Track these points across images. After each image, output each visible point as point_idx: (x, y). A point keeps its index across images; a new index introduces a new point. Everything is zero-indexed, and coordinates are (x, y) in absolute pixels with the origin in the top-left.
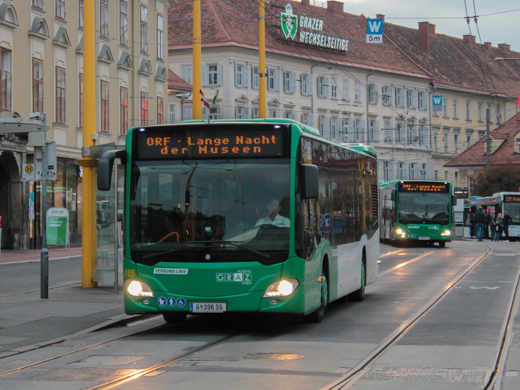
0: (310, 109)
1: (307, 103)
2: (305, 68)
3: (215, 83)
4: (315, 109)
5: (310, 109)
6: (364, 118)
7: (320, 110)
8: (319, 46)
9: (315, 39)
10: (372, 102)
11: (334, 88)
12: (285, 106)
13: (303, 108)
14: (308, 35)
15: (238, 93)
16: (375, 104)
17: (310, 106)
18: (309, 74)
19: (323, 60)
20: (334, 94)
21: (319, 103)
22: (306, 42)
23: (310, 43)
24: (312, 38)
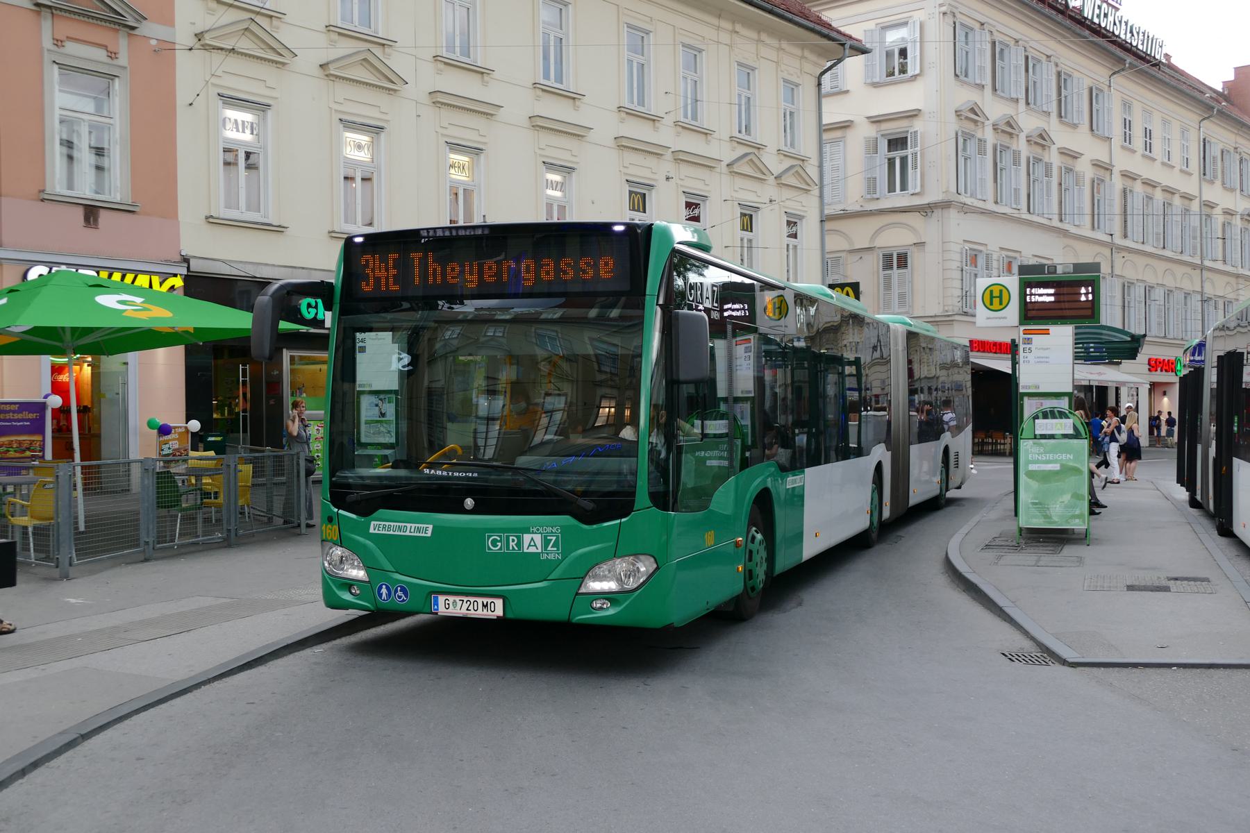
3: (903, 70)
4: (1116, 171)
5: (1108, 168)
6: (1195, 206)
7: (1126, 175)
9: (1111, 18)
10: (1207, 177)
11: (1148, 133)
12: (1064, 152)
14: (1099, 7)
15: (964, 96)
16: (1212, 182)
18: (1106, 89)
20: (1148, 147)
22: (1096, 20)
23: (1103, 25)
24: (1106, 15)
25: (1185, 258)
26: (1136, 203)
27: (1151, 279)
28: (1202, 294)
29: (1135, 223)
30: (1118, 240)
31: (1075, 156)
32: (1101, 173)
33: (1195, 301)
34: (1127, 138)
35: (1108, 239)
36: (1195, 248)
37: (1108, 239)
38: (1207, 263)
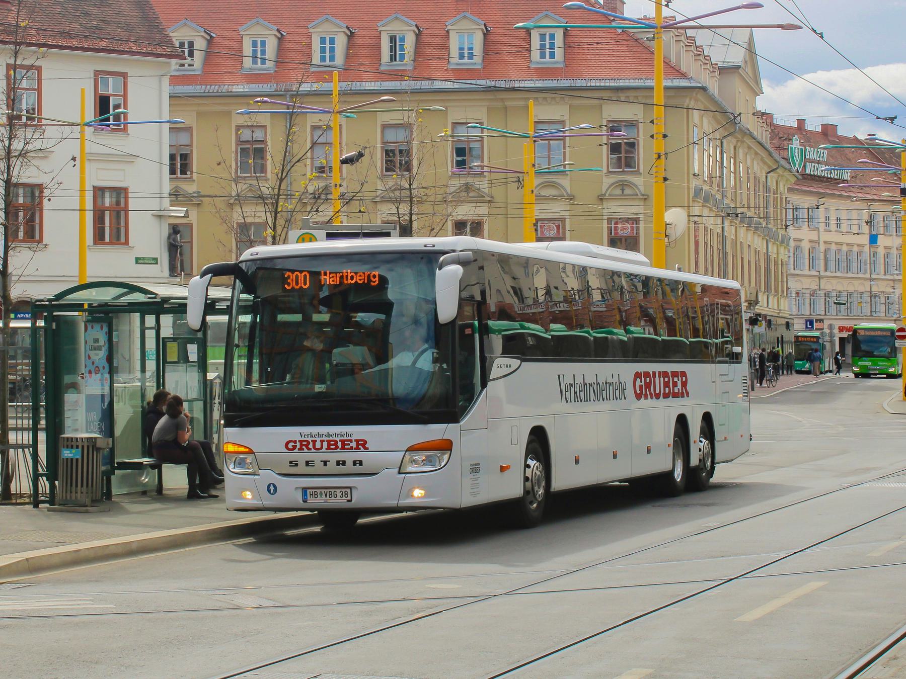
0: (817, 242)
1: (813, 236)
2: (812, 201)
5: (817, 242)
7: (825, 242)
8: (824, 177)
13: (811, 241)
17: (816, 238)
19: (828, 191)
21: (824, 237)
25: (861, 275)
26: (832, 256)
27: (840, 288)
28: (871, 292)
29: (832, 265)
30: (822, 273)
31: (800, 240)
32: (813, 245)
33: (867, 297)
34: (827, 225)
35: (817, 274)
36: (866, 270)
37: (817, 274)
38: (873, 276)
